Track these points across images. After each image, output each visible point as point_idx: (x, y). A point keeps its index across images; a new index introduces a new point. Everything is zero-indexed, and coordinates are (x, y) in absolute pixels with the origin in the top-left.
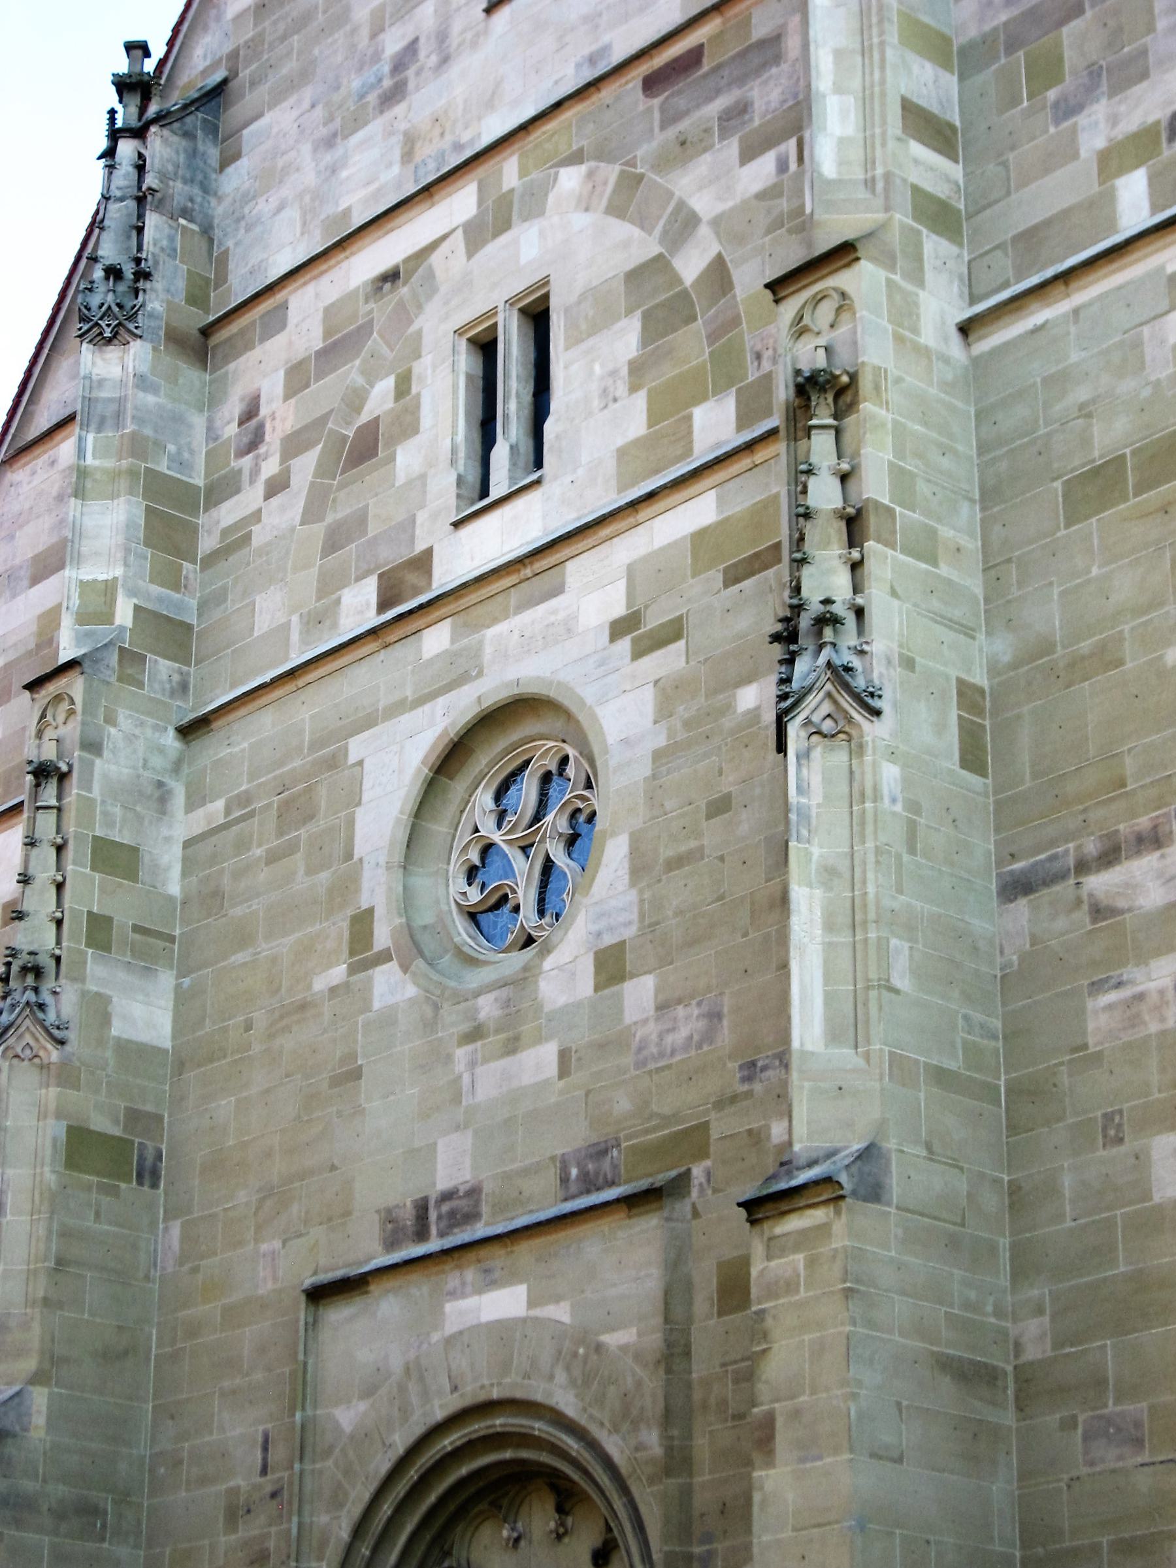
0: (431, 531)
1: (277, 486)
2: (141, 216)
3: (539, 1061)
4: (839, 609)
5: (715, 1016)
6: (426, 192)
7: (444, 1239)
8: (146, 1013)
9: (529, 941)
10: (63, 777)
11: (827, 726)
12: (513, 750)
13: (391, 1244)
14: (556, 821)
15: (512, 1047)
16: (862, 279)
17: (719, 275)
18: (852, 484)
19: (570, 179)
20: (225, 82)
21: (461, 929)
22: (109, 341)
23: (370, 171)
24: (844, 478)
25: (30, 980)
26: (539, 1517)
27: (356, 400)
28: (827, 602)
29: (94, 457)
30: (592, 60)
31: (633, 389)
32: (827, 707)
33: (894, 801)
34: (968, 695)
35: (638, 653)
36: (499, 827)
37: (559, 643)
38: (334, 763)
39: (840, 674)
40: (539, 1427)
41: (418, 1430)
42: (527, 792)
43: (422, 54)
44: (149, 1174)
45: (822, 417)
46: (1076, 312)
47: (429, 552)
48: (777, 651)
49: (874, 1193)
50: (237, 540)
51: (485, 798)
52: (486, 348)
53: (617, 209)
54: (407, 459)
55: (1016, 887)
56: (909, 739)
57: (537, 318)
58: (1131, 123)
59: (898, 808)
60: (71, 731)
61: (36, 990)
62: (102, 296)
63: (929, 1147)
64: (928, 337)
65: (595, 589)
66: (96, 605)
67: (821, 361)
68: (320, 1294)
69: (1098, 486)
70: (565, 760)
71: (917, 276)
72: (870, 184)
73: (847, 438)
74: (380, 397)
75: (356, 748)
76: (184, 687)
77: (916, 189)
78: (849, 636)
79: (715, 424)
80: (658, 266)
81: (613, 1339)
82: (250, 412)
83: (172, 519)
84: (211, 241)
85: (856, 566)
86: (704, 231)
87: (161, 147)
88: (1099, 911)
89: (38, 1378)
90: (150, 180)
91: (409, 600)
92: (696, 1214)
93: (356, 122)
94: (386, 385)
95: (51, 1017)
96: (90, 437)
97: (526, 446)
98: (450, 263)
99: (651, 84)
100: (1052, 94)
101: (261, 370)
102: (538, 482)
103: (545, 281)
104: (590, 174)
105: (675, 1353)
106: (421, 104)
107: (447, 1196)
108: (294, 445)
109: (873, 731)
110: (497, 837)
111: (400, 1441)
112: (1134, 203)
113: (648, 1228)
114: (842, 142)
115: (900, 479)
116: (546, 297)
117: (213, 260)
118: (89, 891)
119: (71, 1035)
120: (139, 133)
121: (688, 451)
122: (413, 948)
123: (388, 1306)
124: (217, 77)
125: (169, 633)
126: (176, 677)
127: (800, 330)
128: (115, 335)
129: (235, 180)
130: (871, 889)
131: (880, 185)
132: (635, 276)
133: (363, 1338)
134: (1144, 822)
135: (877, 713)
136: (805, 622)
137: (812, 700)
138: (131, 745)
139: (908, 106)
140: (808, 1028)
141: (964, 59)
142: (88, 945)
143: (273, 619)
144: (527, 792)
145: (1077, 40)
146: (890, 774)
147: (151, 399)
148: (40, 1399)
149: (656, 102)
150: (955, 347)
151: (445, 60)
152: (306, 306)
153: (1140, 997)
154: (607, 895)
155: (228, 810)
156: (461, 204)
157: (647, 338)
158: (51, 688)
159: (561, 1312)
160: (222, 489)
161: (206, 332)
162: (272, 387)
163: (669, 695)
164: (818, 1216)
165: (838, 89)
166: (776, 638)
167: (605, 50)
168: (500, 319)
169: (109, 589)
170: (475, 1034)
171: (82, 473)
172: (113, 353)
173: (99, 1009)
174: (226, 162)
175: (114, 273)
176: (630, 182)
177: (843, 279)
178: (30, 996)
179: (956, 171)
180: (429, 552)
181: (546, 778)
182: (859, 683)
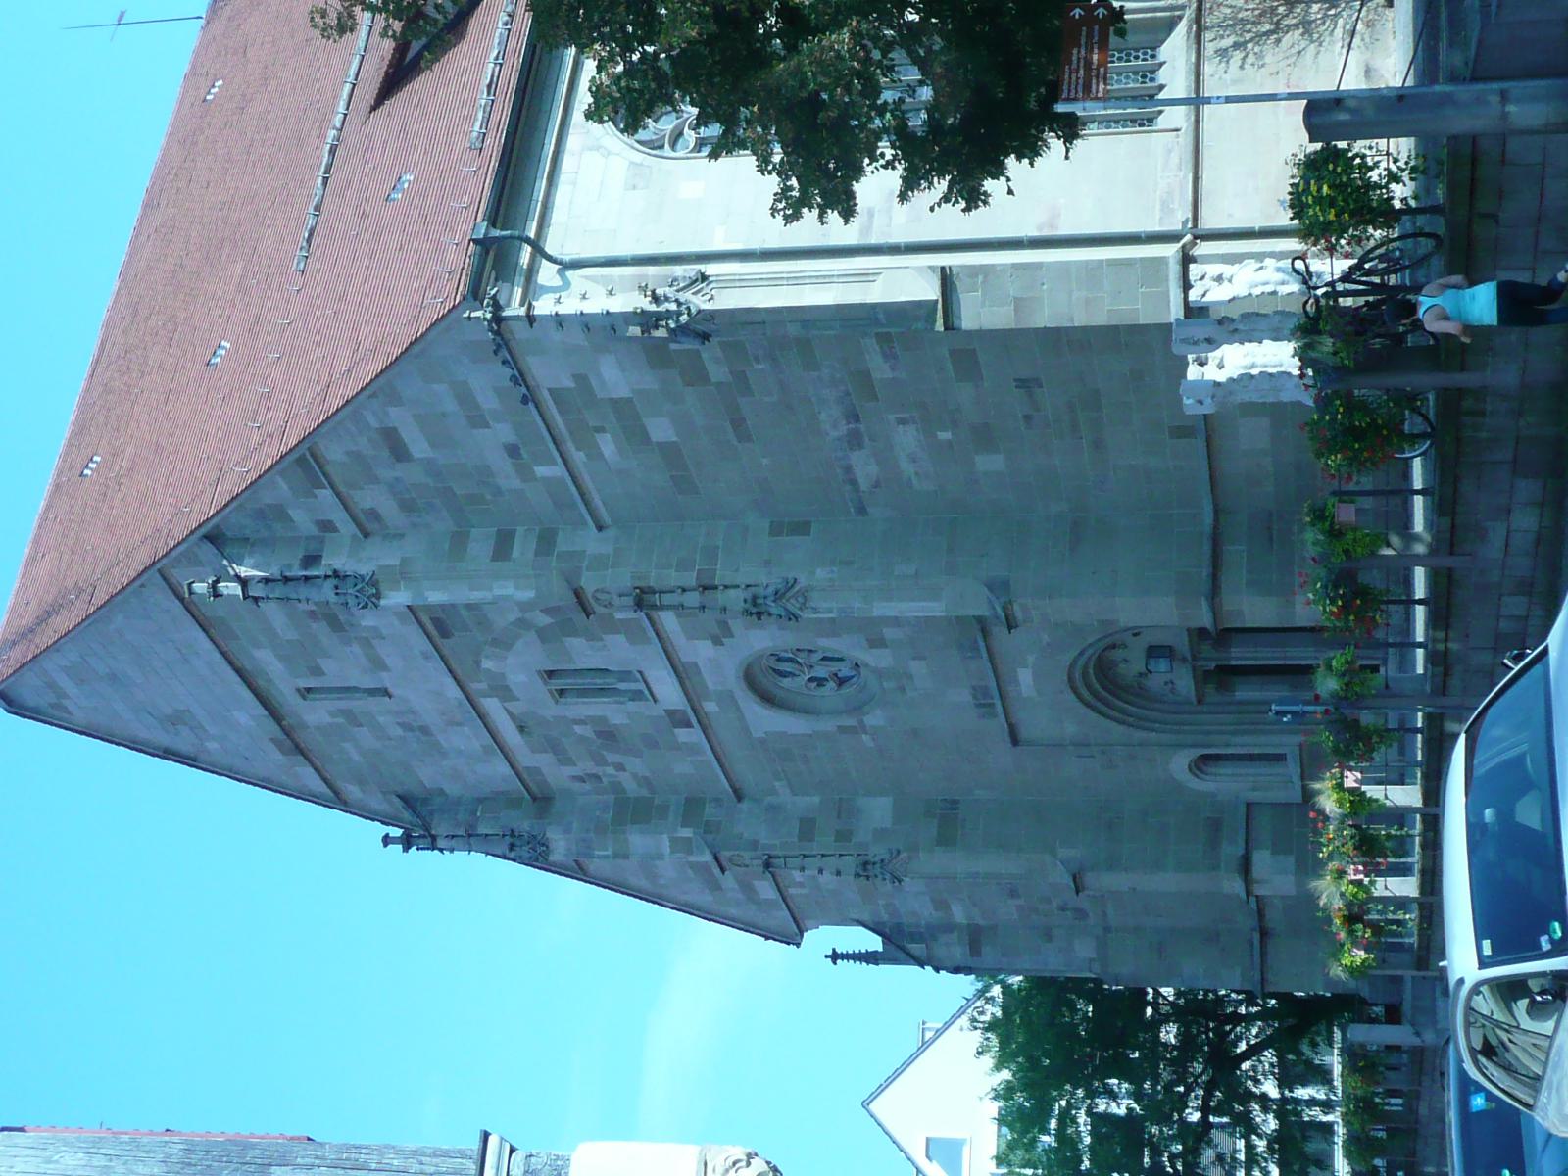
0: (657, 711)
1: (620, 768)
2: (478, 835)
4: (748, 594)
6: (482, 717)
7: (995, 697)
8: (878, 810)
9: (856, 665)
10: (770, 857)
13: (994, 716)
15: (910, 677)
16: (589, 583)
19: (487, 664)
20: (399, 796)
22: (547, 847)
23: (468, 739)
24: (684, 590)
25: (870, 867)
26: (1118, 654)
27: (582, 739)
28: (745, 601)
29: (606, 850)
30: (426, 656)
34: (776, 530)
37: (721, 664)
38: (762, 741)
39: (778, 595)
40: (1081, 662)
41: (1079, 704)
44: (953, 804)
47: (666, 710)
49: (1005, 585)
50: (646, 782)
51: (786, 682)
52: (562, 692)
55: (862, 510)
57: (551, 674)
60: (747, 855)
61: (874, 864)
62: (525, 851)
64: (608, 549)
65: (699, 652)
66: (681, 846)
68: (1015, 741)
76: (717, 800)
78: (761, 591)
82: (581, 780)
83: (634, 811)
84: (486, 798)
85: (726, 587)
86: (528, 616)
87: (440, 829)
88: (877, 485)
90: (461, 832)
94: (578, 729)
95: (886, 856)
96: (597, 852)
98: (517, 708)
99: (445, 633)
101: (557, 776)
102: (640, 673)
103: (539, 672)
107: (975, 697)
108: (601, 761)
109: (803, 582)
111: (1083, 710)
114: (517, 588)
115: (683, 566)
116: (545, 672)
118: (825, 841)
120: (434, 838)
122: (856, 709)
123: (1021, 716)
124: (397, 800)
125: (692, 808)
126: (713, 804)
128: (543, 845)
129: (453, 789)
133: (1037, 723)
137: (789, 606)
138: (749, 824)
142: (850, 841)
147: (575, 825)
150: (611, 533)
152: (526, 758)
153: (917, 474)
155: (780, 780)
156: (492, 705)
158: (724, 864)
159: (1031, 659)
160: (617, 788)
164: (1016, 607)
165: (490, 589)
169: (674, 841)
170: (902, 689)
171: (616, 856)
173: (880, 834)
174: (441, 792)
175: (512, 847)
176: (495, 642)
178: (878, 866)
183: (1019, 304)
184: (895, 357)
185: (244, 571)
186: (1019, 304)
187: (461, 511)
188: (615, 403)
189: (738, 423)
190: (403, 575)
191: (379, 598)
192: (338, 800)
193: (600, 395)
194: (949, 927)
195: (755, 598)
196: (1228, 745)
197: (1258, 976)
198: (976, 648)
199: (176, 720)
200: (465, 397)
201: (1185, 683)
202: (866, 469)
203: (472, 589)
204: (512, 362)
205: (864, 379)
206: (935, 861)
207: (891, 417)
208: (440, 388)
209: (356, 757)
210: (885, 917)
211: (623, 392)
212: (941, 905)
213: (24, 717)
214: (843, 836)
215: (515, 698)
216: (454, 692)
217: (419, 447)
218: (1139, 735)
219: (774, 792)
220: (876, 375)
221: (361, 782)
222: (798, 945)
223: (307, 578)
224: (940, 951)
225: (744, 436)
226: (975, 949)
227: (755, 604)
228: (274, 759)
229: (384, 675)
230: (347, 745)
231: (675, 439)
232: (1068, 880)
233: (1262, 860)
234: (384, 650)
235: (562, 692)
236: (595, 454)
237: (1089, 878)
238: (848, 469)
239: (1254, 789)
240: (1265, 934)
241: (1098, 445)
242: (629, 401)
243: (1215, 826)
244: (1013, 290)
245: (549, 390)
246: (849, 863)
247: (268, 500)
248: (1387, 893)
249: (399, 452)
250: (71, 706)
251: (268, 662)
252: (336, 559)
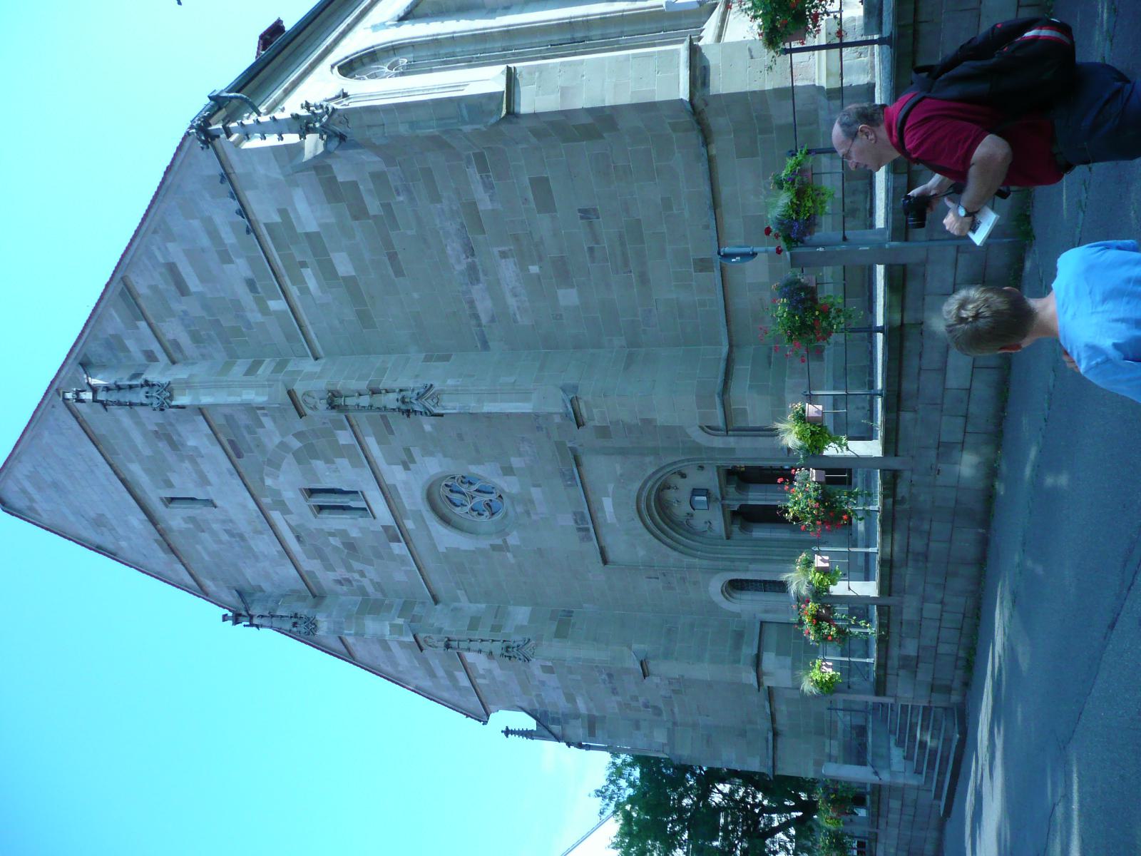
1: (362, 574)
2: (278, 616)
3: (536, 493)
5: (523, 439)
6: (272, 526)
7: (589, 523)
8: (521, 614)
9: (500, 496)
10: (449, 640)
11: (435, 401)
12: (442, 500)
14: (464, 488)
15: (532, 502)
16: (299, 388)
17: (299, 435)
18: (362, 393)
20: (236, 591)
21: (496, 517)
22: (316, 626)
23: (265, 545)
24: (360, 395)
25: (510, 650)
27: (335, 548)
28: (397, 400)
29: (351, 630)
30: (232, 474)
31: (333, 462)
32: (430, 401)
33: (458, 381)
34: (428, 359)
35: (413, 461)
36: (466, 506)
37: (410, 484)
39: (419, 396)
40: (645, 494)
41: (645, 531)
42: (455, 497)
43: (229, 528)
44: (569, 613)
45: (341, 401)
46: (311, 324)
47: (382, 526)
48: (412, 416)
49: (575, 388)
50: (378, 586)
51: (457, 510)
52: (321, 508)
53: (278, 467)
54: (354, 533)
55: (485, 345)
56: (441, 377)
57: (312, 492)
58: (254, 306)
59: (460, 380)
60: (435, 637)
61: (513, 648)
62: (302, 628)
63: (562, 372)
64: (318, 369)
65: (395, 475)
67: (324, 401)
69: (365, 318)
70: (446, 485)
71: (299, 372)
72: (270, 386)
73: (347, 394)
74: (334, 541)
75: (441, 549)
76: (423, 603)
77: (272, 373)
78: (408, 394)
79: (345, 437)
80: (296, 454)
81: (618, 469)
83: (372, 606)
84: (286, 595)
85: (387, 392)
86: (285, 440)
87: (256, 610)
88: (493, 320)
89: (630, 648)
90: (266, 613)
91: (398, 533)
92: (581, 445)
93: (250, 549)
95: (521, 643)
96: (346, 632)
97: (351, 496)
98: (294, 519)
99: (239, 456)
100: (244, 330)
101: (326, 578)
102: (362, 492)
103: (300, 490)
104: (267, 475)
105: (623, 452)
106: (244, 527)
107: (576, 522)
108: (349, 568)
109: (437, 386)
110: (469, 506)
111: (649, 536)
112: (278, 305)
113: (585, 460)
114: (257, 394)
116: (305, 489)
117: (293, 594)
119: (527, 637)
120: (251, 617)
121: (353, 445)
122: (502, 532)
123: (608, 541)
125: (406, 608)
126: (420, 605)
127: (314, 408)
128: (314, 624)
129: (266, 586)
130: (484, 388)
131: (271, 383)
132: (299, 461)
133: (619, 547)
134: (466, 306)
135: (431, 385)
136: (403, 407)
137: (427, 405)
138: (440, 619)
139: (246, 374)
140: (525, 407)
141: (233, 357)
142: (500, 632)
143: (403, 575)
144: (455, 497)
145: (227, 321)
146: (450, 382)
147: (334, 613)
148: (635, 646)
149: (245, 454)
150: (322, 361)
151: (231, 521)
152: (308, 565)
153: (518, 308)
154: (485, 472)
155: (461, 589)
156: (276, 516)
157: (316, 457)
158: (422, 643)
159: (611, 487)
160: (362, 591)
161: (314, 596)
162: (331, 576)
163: (427, 452)
164: (582, 405)
165: (240, 396)
166: (408, 416)
167: (229, 470)
168: (312, 504)
169: (392, 626)
170: (528, 513)
171: (356, 634)
172: (320, 625)
173: (520, 629)
174: (261, 590)
175: (295, 625)
176: (270, 463)
177: (299, 394)
178: (515, 650)
179: (268, 360)
180: (382, 526)
181: (451, 491)
182: (422, 391)
183: (564, 91)
184: (492, 187)
185: (94, 381)
186: (564, 91)
187: (225, 337)
188: (308, 235)
189: (393, 257)
190: (187, 385)
191: (171, 400)
192: (201, 591)
193: (299, 230)
194: (577, 716)
195: (403, 398)
196: (747, 570)
197: (770, 763)
198: (573, 478)
199: (99, 522)
200: (214, 234)
201: (719, 524)
202: (484, 306)
203: (229, 395)
204: (235, 195)
205: (472, 206)
206: (552, 649)
207: (496, 250)
208: (196, 223)
209: (206, 558)
210: (537, 706)
211: (312, 227)
212: (570, 698)
213: (13, 515)
214: (496, 628)
215: (289, 512)
216: (252, 505)
217: (194, 284)
218: (687, 560)
219: (457, 599)
220: (481, 207)
221: (213, 579)
222: (485, 723)
223: (131, 387)
224: (570, 732)
225: (399, 273)
226: (592, 733)
227: (403, 402)
228: (160, 558)
229: (209, 488)
230: (199, 547)
231: (354, 274)
232: (638, 666)
233: (769, 660)
234: (206, 467)
235: (321, 508)
236: (304, 290)
237: (652, 666)
238: (471, 303)
239: (766, 611)
240: (776, 734)
241: (644, 279)
242: (318, 234)
243: (739, 636)
244: (560, 82)
245: (266, 225)
246: (497, 648)
247: (111, 332)
248: (851, 593)
249: (183, 289)
250: (40, 511)
251: (136, 471)
252: (153, 376)
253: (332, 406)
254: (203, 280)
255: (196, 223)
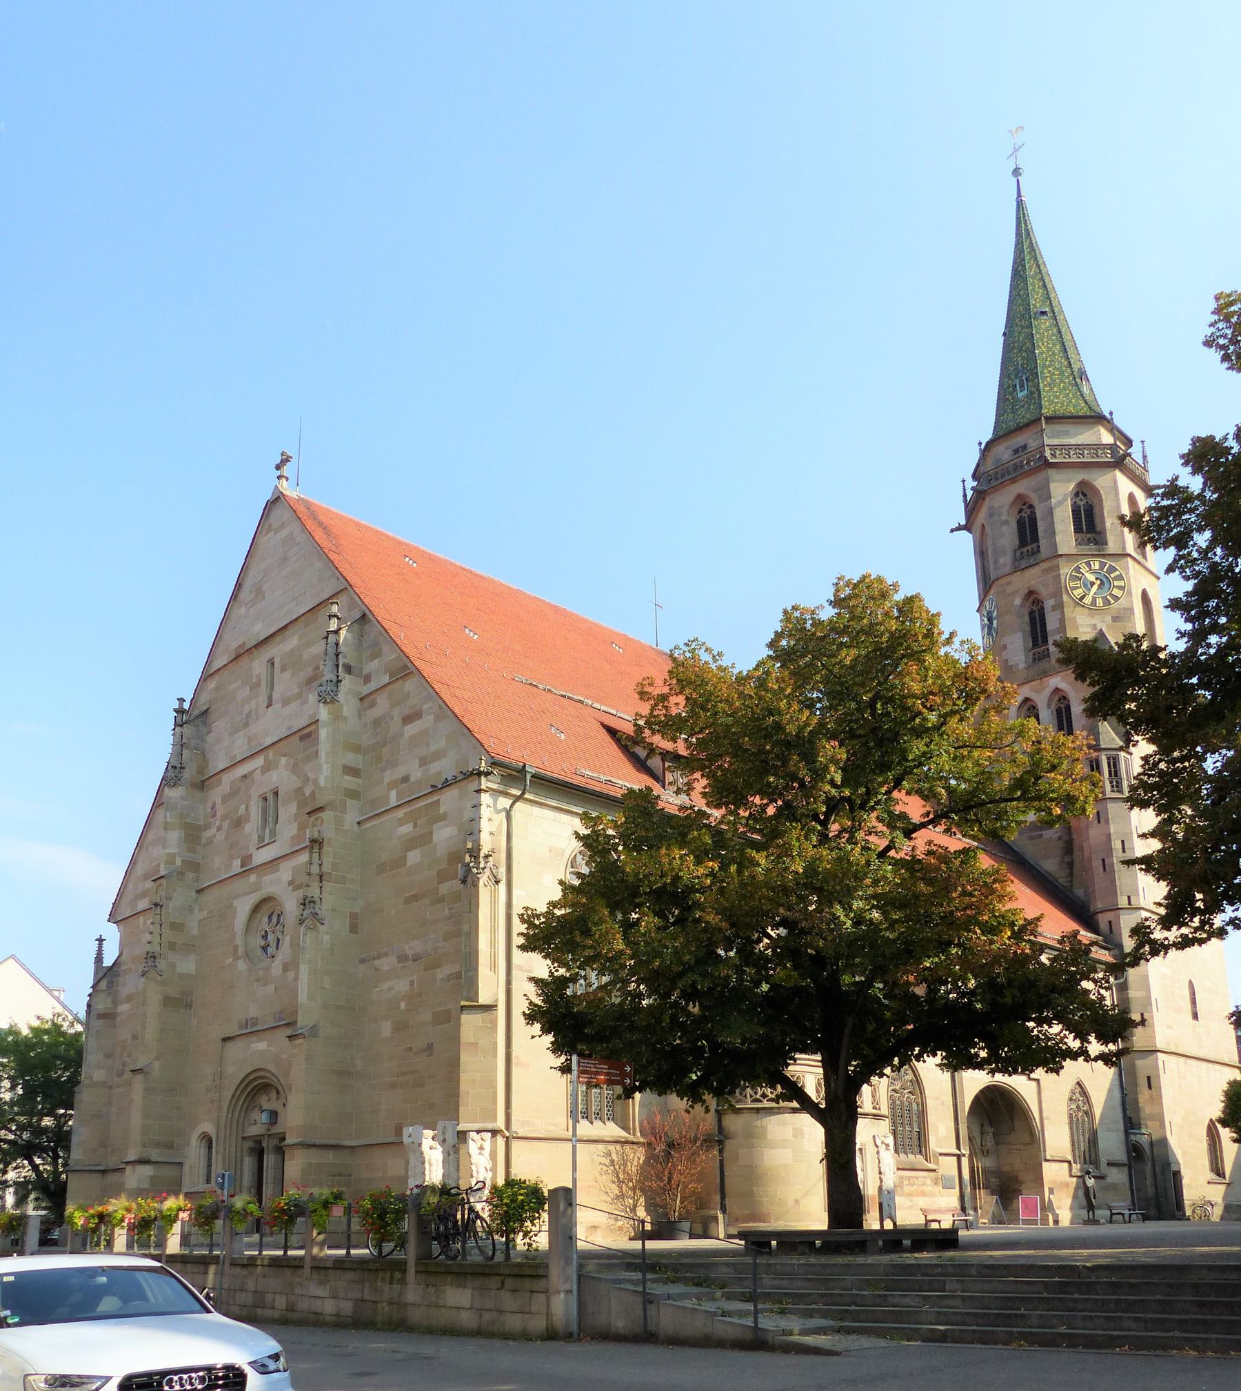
1: (219, 829)
19: (283, 760)
23: (240, 747)
27: (237, 808)
30: (289, 728)
50: (210, 842)
57: (276, 794)
98: (257, 776)
108: (223, 818)
112: (393, 800)
152: (227, 778)
156: (259, 762)
162: (219, 800)
176: (296, 765)
193: (435, 826)
202: (386, 964)
208: (443, 743)
211: (436, 838)
216: (268, 741)
217: (410, 730)
236: (401, 822)
238: (386, 955)
253: (313, 841)
254: (412, 738)
255: (443, 743)
